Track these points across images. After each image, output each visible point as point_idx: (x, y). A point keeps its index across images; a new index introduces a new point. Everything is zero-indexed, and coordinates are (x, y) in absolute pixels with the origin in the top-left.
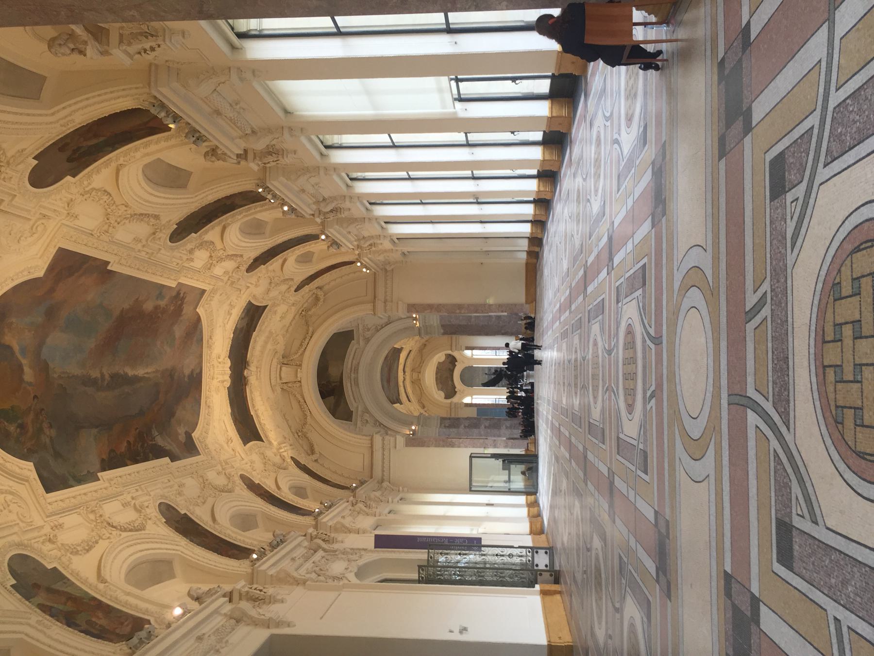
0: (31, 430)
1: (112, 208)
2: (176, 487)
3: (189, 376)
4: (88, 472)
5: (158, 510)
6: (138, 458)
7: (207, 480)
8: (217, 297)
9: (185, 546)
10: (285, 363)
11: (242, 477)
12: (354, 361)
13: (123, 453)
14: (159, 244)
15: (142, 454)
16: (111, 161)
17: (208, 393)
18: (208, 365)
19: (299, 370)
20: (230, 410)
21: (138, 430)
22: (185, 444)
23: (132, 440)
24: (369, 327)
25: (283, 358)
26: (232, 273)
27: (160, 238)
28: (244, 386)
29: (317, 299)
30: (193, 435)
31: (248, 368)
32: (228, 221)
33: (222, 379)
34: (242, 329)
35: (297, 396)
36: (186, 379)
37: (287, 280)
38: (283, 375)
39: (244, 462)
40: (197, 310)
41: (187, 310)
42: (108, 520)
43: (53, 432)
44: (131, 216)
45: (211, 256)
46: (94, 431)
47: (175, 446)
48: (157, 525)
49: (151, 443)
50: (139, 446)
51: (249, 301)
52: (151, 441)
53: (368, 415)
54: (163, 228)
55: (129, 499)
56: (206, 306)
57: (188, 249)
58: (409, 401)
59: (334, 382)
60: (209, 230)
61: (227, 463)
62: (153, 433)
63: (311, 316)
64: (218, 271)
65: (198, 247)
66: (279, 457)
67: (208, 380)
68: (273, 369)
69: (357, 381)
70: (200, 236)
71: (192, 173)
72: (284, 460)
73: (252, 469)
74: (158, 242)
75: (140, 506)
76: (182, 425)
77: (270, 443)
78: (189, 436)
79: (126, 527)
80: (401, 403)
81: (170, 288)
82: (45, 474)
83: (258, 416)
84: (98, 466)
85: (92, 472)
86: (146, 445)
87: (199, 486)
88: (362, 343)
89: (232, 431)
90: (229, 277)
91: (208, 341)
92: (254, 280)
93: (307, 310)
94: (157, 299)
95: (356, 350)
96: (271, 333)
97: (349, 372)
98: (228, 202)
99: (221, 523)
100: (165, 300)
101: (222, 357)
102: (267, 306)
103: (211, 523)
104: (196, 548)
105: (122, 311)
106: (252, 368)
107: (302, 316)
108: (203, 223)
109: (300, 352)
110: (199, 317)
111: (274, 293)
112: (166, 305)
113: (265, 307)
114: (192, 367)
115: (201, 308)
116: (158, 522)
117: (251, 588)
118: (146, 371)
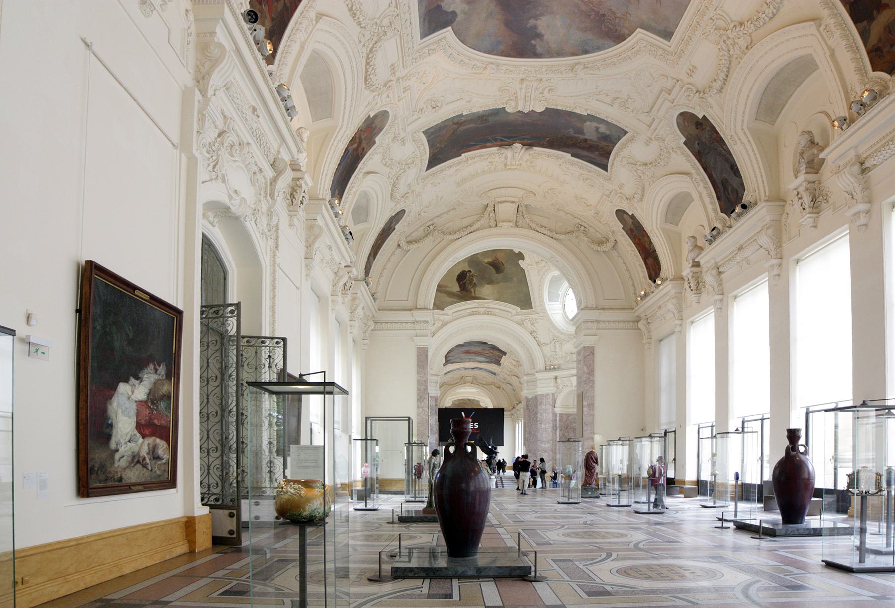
3: (535, 27)
10: (519, 209)
12: (497, 311)
17: (504, 68)
19: (511, 224)
24: (535, 325)
29: (600, 243)
31: (524, 149)
34: (581, 131)
36: (532, 22)
38: (504, 205)
40: (639, 30)
51: (626, 133)
53: (439, 325)
58: (445, 374)
59: (475, 292)
69: (475, 314)
80: (444, 365)
83: (459, 163)
88: (518, 318)
93: (585, 232)
95: (509, 312)
97: (486, 306)
107: (578, 227)
109: (533, 226)
113: (605, 167)
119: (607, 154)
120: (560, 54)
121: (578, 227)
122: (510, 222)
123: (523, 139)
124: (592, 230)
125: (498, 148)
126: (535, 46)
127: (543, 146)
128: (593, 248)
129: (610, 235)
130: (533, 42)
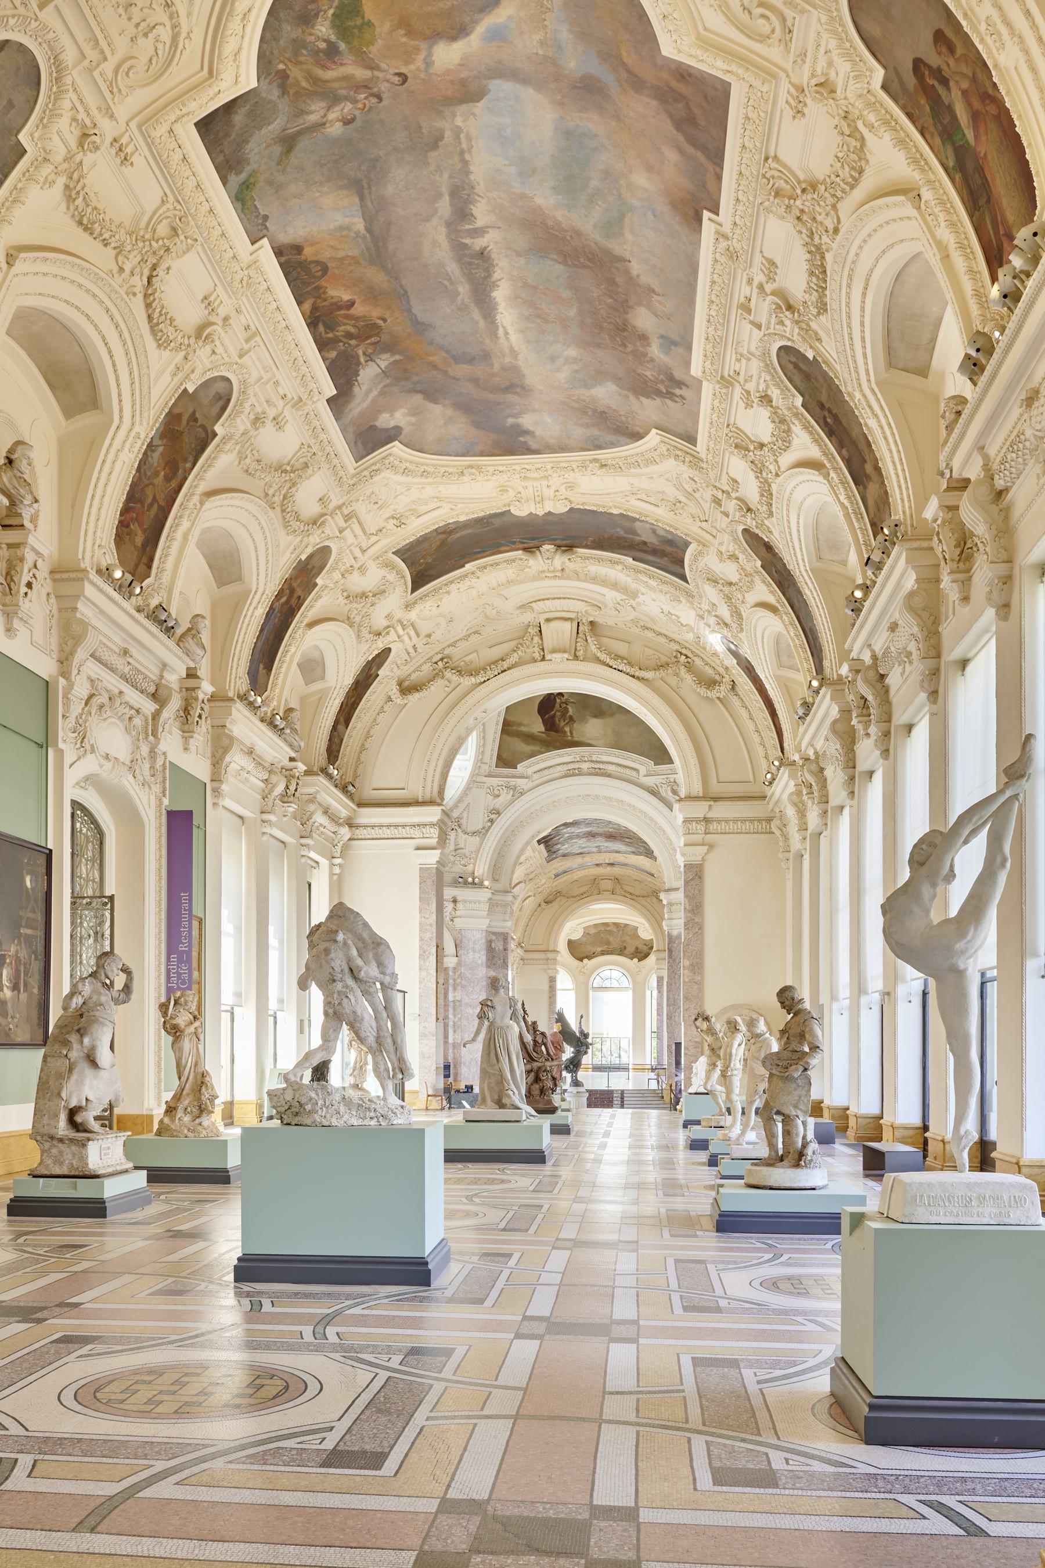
0: (330, 75)
1: (827, 194)
2: (271, 413)
3: (518, 425)
4: (266, 218)
5: (209, 375)
6: (321, 328)
7: (300, 476)
8: (686, 472)
9: (133, 434)
11: (323, 553)
13: (325, 293)
14: (769, 323)
15: (330, 335)
16: (923, 170)
17: (491, 469)
18: (549, 467)
19: (566, 656)
20: (462, 518)
21: (380, 322)
22: (373, 428)
23: (359, 310)
25: (592, 623)
26: (737, 498)
27: (782, 323)
28: (521, 546)
29: (711, 683)
30: (396, 443)
31: (559, 552)
32: (832, 474)
33: (523, 495)
35: (515, 655)
36: (510, 421)
37: (740, 616)
39: (358, 553)
40: (654, 431)
41: (648, 408)
42: (163, 266)
43: (336, 129)
44: (815, 246)
45: (762, 445)
46: (360, 225)
47: (365, 405)
48: (175, 374)
49: (360, 352)
50: (349, 328)
52: (364, 354)
54: (804, 326)
55: (222, 311)
56: (664, 448)
57: (769, 393)
60: (811, 433)
61: (347, 518)
62: (384, 356)
63: (677, 675)
64: (738, 467)
65: (775, 413)
66: (384, 623)
67: (517, 468)
68: (565, 604)
70: (796, 415)
71: (926, 377)
72: (380, 634)
73: (347, 571)
74: (773, 320)
75: (209, 334)
76: (413, 419)
77: (408, 606)
78: (391, 435)
79: (154, 305)
81: (687, 364)
82: (239, 118)
84: (285, 238)
85: (268, 224)
86: (353, 342)
87: (286, 461)
89: (417, 527)
90: (728, 493)
91: (596, 460)
92: (729, 546)
93: (689, 667)
94: (662, 337)
96: (634, 595)
98: (869, 468)
99: (205, 507)
100: (662, 356)
101: (569, 494)
102: (687, 582)
103: (203, 487)
104: (132, 456)
105: (622, 260)
106: (560, 560)
107: (676, 657)
108: (825, 418)
109: (603, 656)
110: (642, 438)
111: (711, 593)
112: (652, 360)
114: (539, 432)
115: (658, 439)
116: (181, 375)
117: (35, 566)
118: (511, 331)
119: (681, 562)
120: (563, 449)
121: (676, 657)
122: (565, 652)
123: (555, 540)
124: (698, 662)
125: (520, 552)
126: (525, 442)
127: (587, 547)
128: (699, 693)
129: (721, 670)
130: (521, 439)
